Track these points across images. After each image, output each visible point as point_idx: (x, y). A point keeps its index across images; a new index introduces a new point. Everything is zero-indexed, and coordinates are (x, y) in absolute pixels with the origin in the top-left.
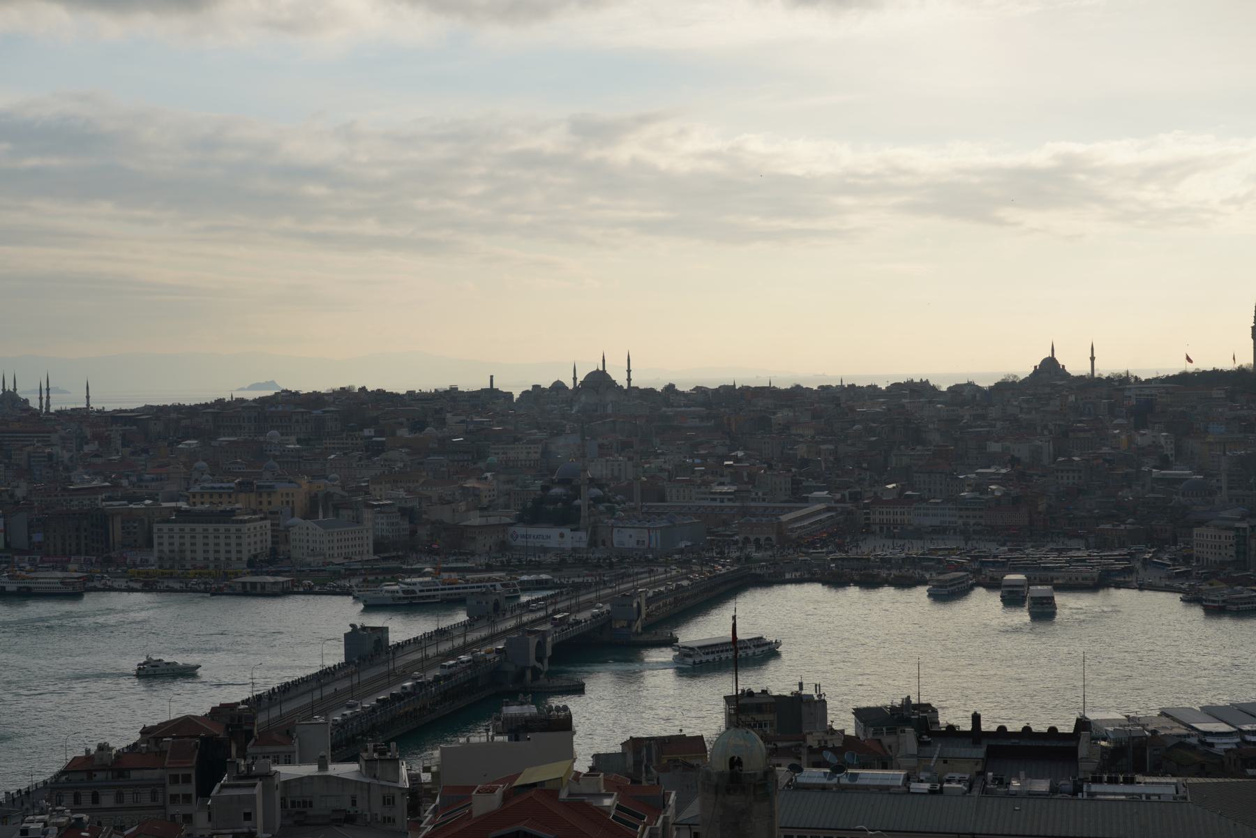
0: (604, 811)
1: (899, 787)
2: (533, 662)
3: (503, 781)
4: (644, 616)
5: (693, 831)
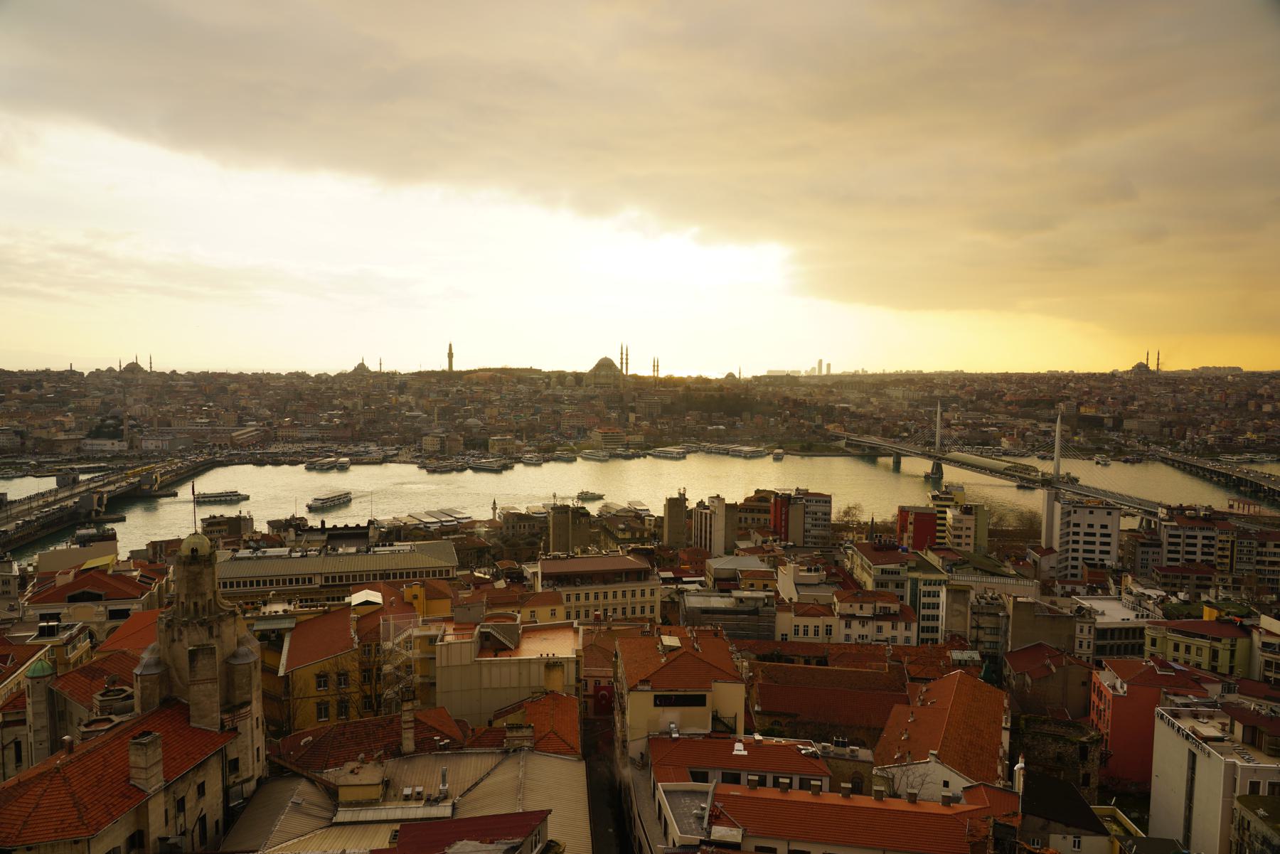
0: (134, 578)
2: (96, 507)
3: (74, 568)
4: (159, 482)
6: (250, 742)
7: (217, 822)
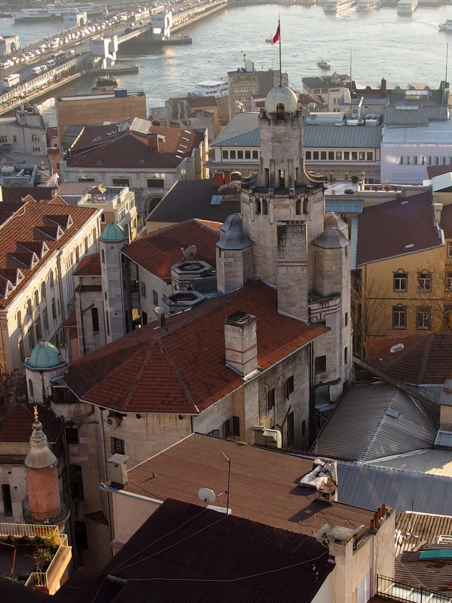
1: (340, 122)
4: (171, 25)
5: (222, 150)
6: (338, 341)
7: (304, 423)
